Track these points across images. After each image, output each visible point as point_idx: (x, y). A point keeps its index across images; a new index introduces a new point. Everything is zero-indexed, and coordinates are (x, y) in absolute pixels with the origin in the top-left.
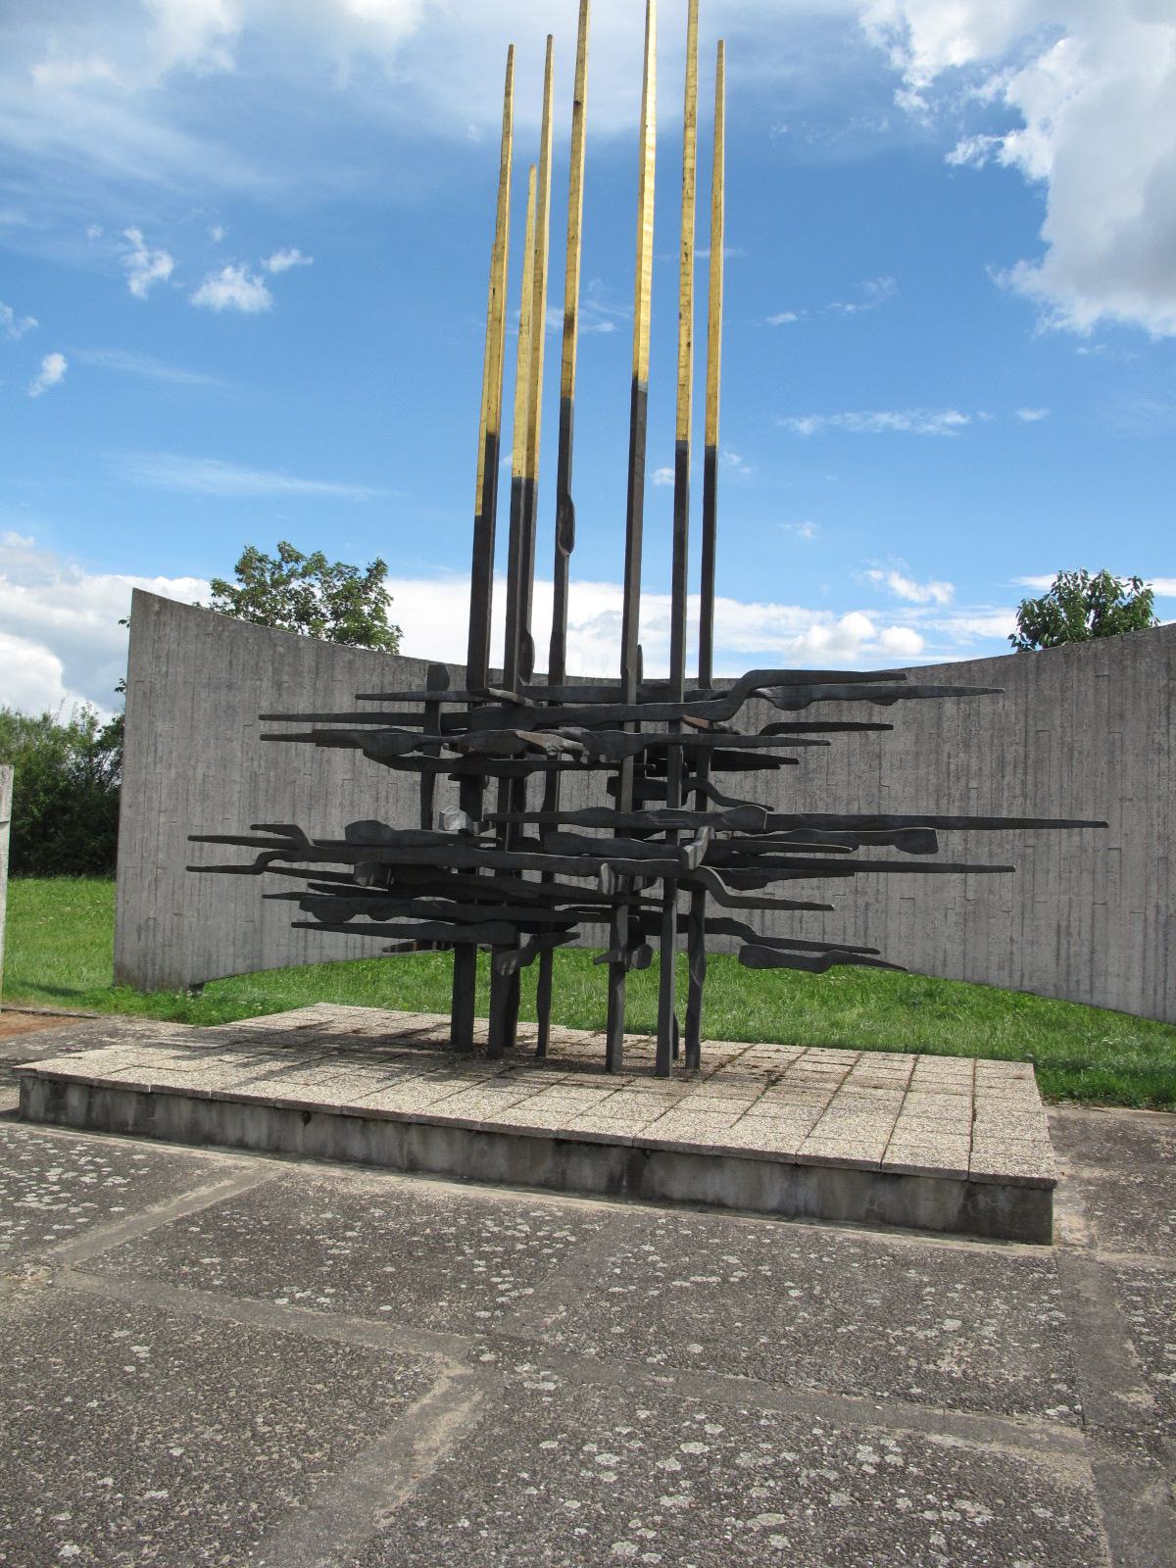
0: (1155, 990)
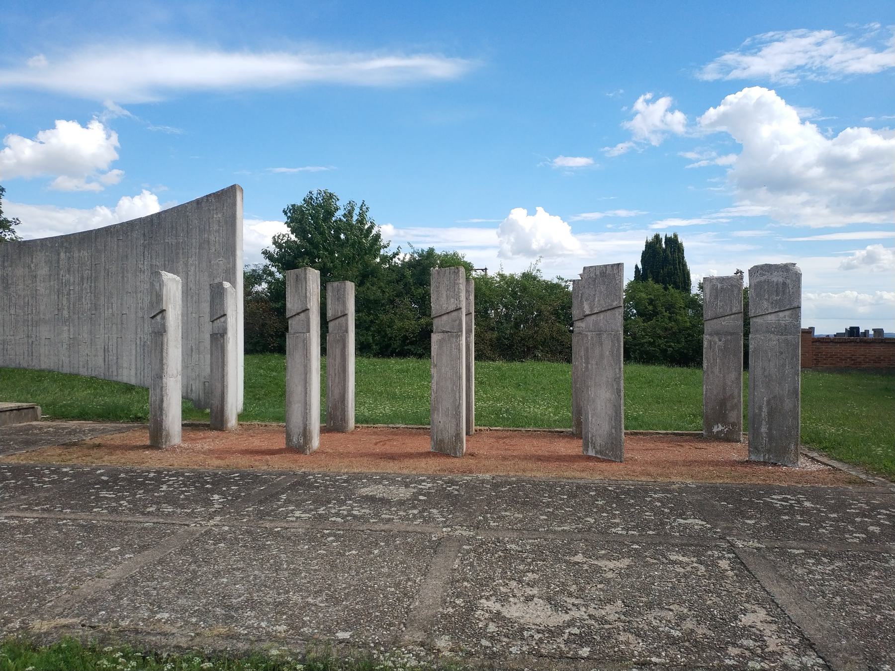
0: (140, 374)
